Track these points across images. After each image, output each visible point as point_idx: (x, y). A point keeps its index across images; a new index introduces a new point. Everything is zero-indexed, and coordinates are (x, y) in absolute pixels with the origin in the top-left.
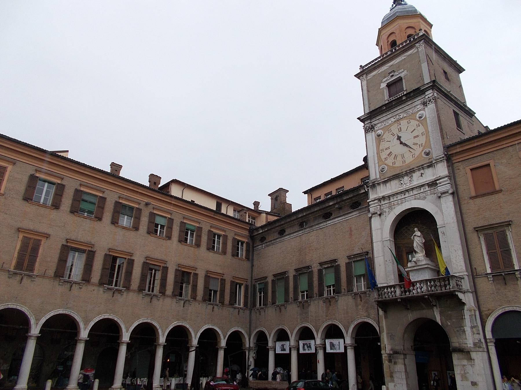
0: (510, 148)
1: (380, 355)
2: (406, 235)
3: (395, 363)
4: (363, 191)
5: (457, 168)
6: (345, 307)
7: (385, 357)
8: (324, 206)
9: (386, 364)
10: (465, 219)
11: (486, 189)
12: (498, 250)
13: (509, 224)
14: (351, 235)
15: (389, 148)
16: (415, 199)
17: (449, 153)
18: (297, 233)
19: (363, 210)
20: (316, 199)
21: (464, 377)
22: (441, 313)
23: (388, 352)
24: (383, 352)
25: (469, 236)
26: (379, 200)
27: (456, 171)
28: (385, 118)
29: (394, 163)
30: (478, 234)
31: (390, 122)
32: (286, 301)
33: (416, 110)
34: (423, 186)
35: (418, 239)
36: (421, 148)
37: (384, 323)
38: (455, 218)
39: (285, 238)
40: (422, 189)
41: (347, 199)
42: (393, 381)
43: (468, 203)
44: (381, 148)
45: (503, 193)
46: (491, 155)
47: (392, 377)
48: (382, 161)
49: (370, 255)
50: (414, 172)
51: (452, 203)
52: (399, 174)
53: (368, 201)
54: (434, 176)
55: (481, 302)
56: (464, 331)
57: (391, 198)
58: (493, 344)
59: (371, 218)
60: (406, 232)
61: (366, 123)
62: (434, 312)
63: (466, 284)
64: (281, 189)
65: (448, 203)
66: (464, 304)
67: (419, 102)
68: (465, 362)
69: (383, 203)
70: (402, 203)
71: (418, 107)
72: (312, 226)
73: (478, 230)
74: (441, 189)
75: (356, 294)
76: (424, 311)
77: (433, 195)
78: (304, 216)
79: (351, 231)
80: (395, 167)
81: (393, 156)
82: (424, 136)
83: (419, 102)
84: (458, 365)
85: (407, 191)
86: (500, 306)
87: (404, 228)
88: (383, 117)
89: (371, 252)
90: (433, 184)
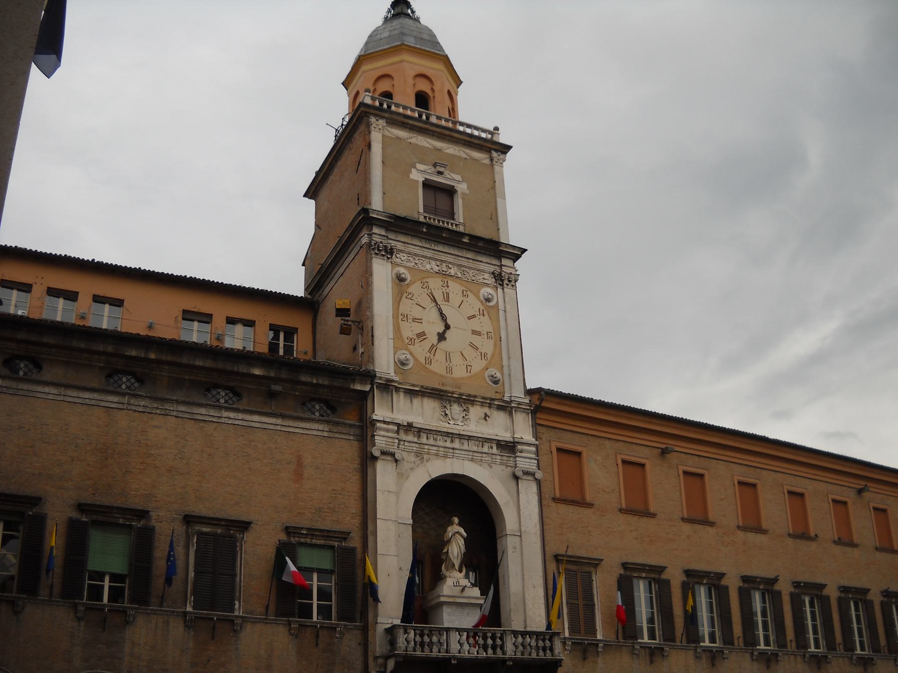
0: (607, 442)
4: (358, 387)
8: (229, 367)
12: (581, 603)
14: (298, 475)
16: (472, 460)
17: (544, 404)
18: (95, 396)
19: (341, 429)
28: (417, 251)
31: (428, 267)
33: (480, 278)
36: (484, 363)
39: (40, 388)
40: (486, 445)
50: (473, 405)
57: (424, 436)
59: (375, 459)
69: (403, 436)
70: (445, 457)
72: (163, 400)
77: (503, 467)
78: (147, 360)
79: (300, 464)
80: (430, 371)
81: (427, 345)
83: (492, 269)
85: (461, 437)
88: (415, 246)
90: (509, 447)
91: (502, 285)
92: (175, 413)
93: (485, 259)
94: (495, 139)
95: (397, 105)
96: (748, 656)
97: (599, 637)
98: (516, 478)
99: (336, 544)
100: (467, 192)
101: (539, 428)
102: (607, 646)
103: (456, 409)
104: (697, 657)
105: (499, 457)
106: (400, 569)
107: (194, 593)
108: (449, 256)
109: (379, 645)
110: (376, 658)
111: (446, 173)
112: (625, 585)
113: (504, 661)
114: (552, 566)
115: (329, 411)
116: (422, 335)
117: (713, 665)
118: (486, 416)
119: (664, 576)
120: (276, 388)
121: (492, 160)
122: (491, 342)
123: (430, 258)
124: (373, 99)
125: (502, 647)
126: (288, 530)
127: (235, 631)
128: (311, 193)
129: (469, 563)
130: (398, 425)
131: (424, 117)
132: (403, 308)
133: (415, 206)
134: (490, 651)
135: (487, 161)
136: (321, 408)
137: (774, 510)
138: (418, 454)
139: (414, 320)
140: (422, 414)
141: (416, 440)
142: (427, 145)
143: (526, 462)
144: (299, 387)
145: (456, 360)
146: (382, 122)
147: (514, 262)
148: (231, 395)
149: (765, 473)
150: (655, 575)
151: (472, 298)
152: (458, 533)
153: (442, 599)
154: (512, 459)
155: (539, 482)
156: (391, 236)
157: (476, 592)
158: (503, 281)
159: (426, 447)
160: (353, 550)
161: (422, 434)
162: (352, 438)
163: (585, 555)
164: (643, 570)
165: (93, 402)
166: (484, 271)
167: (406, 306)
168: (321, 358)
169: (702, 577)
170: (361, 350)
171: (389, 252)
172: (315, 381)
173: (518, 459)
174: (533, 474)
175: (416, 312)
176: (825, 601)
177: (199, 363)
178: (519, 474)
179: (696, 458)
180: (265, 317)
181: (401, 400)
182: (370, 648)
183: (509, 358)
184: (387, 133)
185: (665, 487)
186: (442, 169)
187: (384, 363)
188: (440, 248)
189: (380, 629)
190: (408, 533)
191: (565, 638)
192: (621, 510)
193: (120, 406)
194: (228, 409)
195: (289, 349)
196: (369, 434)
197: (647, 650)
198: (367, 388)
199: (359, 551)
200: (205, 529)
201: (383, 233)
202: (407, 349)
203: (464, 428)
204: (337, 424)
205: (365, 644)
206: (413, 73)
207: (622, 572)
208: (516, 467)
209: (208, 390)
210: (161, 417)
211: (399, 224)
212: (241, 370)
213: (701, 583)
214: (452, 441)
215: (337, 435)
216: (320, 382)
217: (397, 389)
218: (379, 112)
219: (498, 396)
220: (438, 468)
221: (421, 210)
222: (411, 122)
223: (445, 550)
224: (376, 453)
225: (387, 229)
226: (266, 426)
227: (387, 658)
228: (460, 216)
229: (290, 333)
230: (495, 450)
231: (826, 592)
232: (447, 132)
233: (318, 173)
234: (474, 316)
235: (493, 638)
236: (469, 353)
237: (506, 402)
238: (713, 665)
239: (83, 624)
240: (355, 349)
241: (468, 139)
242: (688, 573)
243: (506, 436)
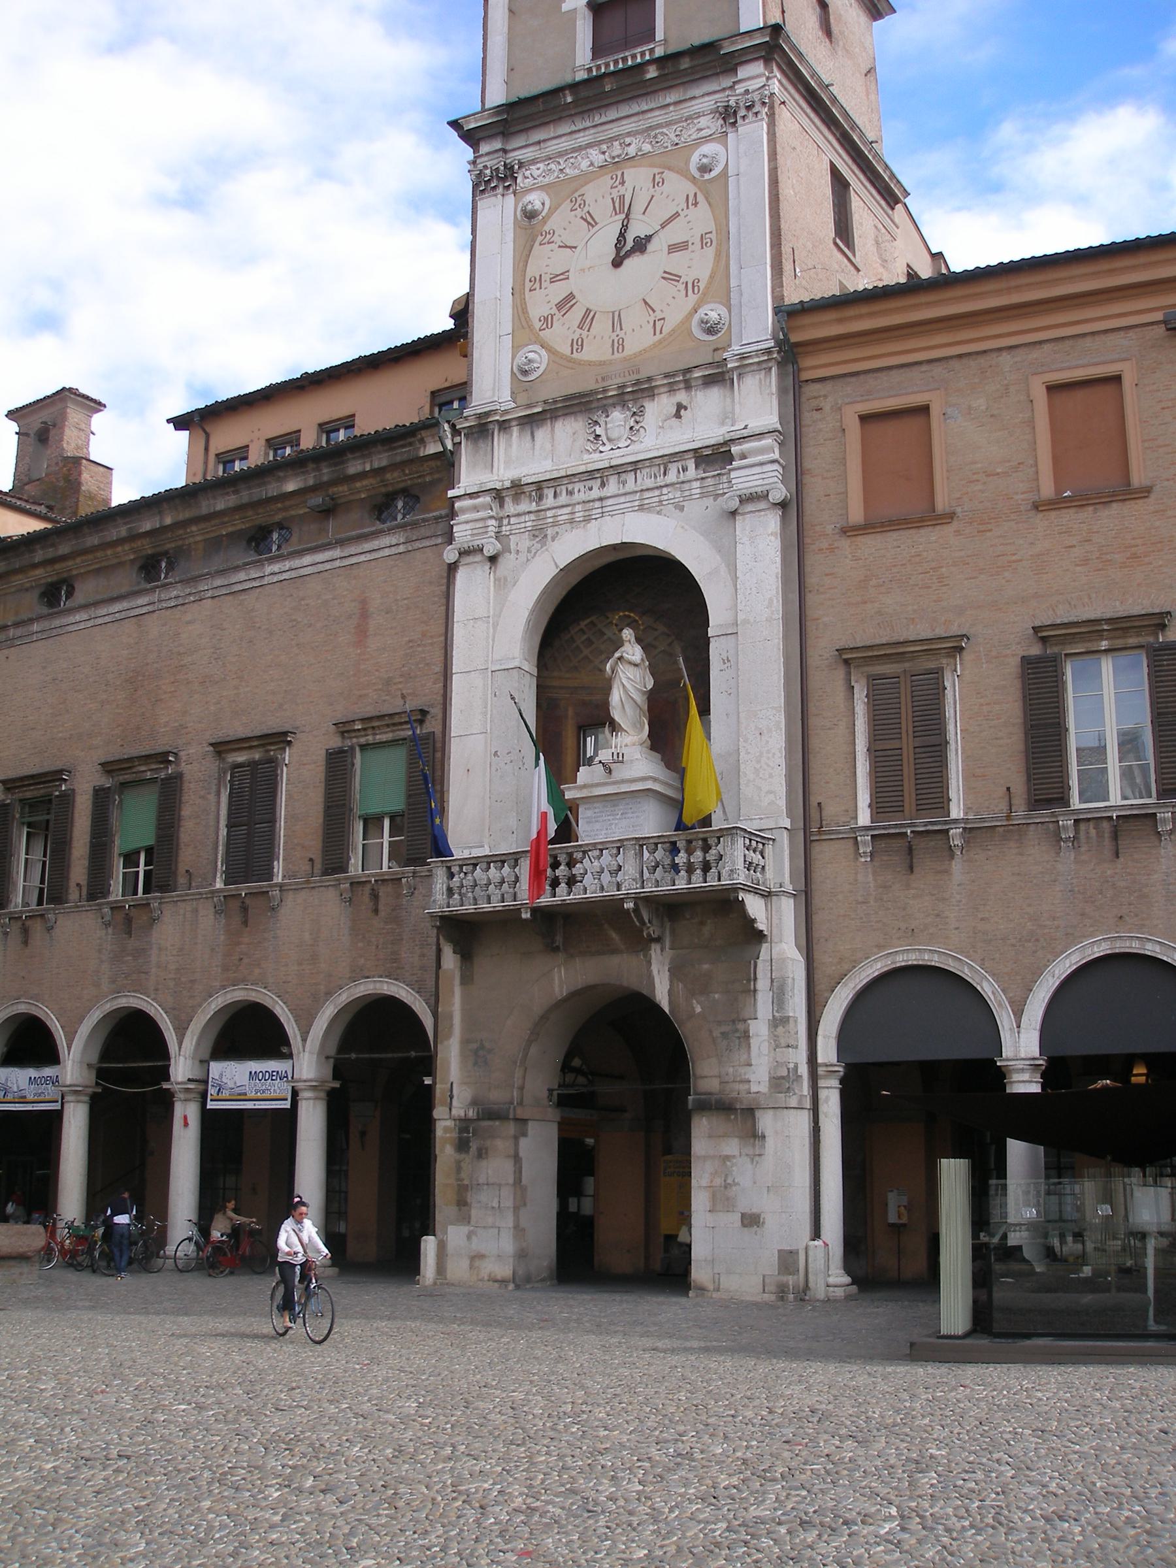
0: (1005, 358)
1: (428, 1124)
2: (586, 652)
3: (481, 1154)
4: (433, 448)
5: (814, 403)
6: (307, 936)
7: (446, 1129)
9: (445, 1154)
10: (811, 613)
11: (904, 498)
12: (907, 744)
13: (955, 647)
14: (362, 633)
15: (563, 276)
16: (641, 508)
17: (794, 338)
18: (125, 605)
19: (423, 531)
20: (226, 459)
21: (722, 1199)
22: (676, 972)
23: (458, 1112)
24: (439, 1112)
25: (816, 679)
26: (498, 495)
27: (808, 417)
28: (564, 144)
29: (578, 345)
30: (849, 674)
32: (53, 892)
33: (691, 134)
35: (629, 677)
36: (693, 298)
37: (455, 1003)
38: (778, 605)
39: (71, 619)
41: (363, 475)
42: (466, 1219)
43: (832, 549)
44: (532, 271)
45: (955, 525)
46: (938, 370)
47: (462, 1203)
49: (432, 725)
50: (652, 397)
51: (776, 543)
52: (592, 393)
53: (451, 493)
54: (723, 423)
55: (819, 932)
56: (746, 1036)
57: (549, 493)
58: (835, 1083)
59: (452, 568)
60: (589, 642)
61: (485, 148)
62: (649, 963)
63: (779, 867)
64: (65, 395)
65: (762, 543)
66: (760, 936)
67: (707, 104)
68: (731, 1147)
70: (587, 519)
71: (704, 122)
72: (195, 579)
73: (848, 659)
74: (744, 479)
75: (356, 884)
76: (614, 961)
77: (709, 501)
78: (164, 529)
79: (364, 615)
80: (579, 363)
81: (577, 314)
82: (710, 252)
84: (705, 1158)
85: (618, 470)
86: (880, 947)
87: (583, 624)
88: (559, 138)
89: (436, 711)
90: (716, 457)
92: (209, 594)
102: (970, 832)
105: (697, 484)
106: (496, 754)
140: (558, 449)
144: (358, 485)
152: (620, 658)
154: (724, 479)
158: (735, 113)
159: (549, 513)
161: (546, 491)
162: (439, 540)
164: (1100, 634)
165: (123, 615)
166: (699, 115)
173: (733, 475)
177: (220, 505)
188: (612, 114)
192: (1036, 507)
193: (150, 608)
197: (1105, 825)
199: (438, 735)
200: (241, 758)
204: (414, 525)
207: (1035, 650)
210: (195, 605)
214: (603, 485)
215: (418, 545)
216: (376, 465)
217: (504, 426)
226: (321, 567)
234: (677, 215)
239: (110, 930)
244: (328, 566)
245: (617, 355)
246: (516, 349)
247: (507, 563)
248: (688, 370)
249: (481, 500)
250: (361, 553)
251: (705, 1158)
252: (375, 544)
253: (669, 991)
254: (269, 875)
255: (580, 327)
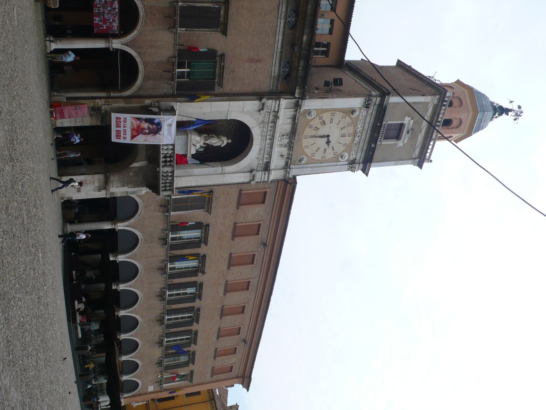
0: (269, 216)
3: (91, 115)
4: (297, 91)
7: (98, 103)
9: (91, 103)
14: (251, 61)
16: (260, 149)
17: (289, 185)
22: (140, 168)
23: (103, 107)
28: (368, 120)
31: (359, 126)
34: (270, 157)
36: (310, 155)
44: (337, 113)
48: (320, 114)
50: (288, 149)
56: (124, 186)
59: (260, 100)
65: (243, 178)
68: (97, 184)
70: (262, 136)
77: (257, 165)
81: (319, 126)
83: (358, 158)
84: (94, 178)
86: (143, 202)
90: (267, 168)
91: (349, 164)
93: (363, 155)
94: (426, 160)
95: (445, 110)
96: (163, 286)
97: (172, 213)
98: (251, 171)
99: (216, 80)
100: (398, 146)
101: (277, 182)
102: (167, 217)
103: (286, 141)
104: (162, 261)
107: (189, 7)
108: (365, 137)
109: (165, 103)
110: (158, 102)
111: (408, 135)
112: (198, 226)
113: (159, 167)
114: (207, 190)
115: (284, 76)
116: (324, 123)
117: (158, 269)
118: (282, 156)
119: (203, 245)
120: (296, 48)
121: (415, 159)
122: (320, 159)
123: (364, 127)
124: (449, 97)
125: (166, 166)
126: (223, 56)
127: (169, 29)
128: (400, 64)
129: (208, 148)
130: (278, 112)
131: (438, 124)
132: (338, 113)
133: (390, 120)
134: (164, 159)
135: (414, 156)
136: (286, 72)
137: (235, 299)
138: (263, 122)
139: (332, 119)
141: (270, 120)
142: (423, 125)
143: (260, 176)
145: (312, 140)
146: (436, 102)
147: (362, 170)
148: (292, 24)
149: (254, 294)
150: (203, 240)
151: (343, 148)
153: (189, 135)
155: (249, 182)
156: (376, 107)
157: (193, 152)
158: (351, 164)
160: (214, 90)
163: (213, 206)
164: (205, 235)
167: (339, 115)
168: (313, 70)
169: (202, 264)
170: (316, 92)
171: (367, 106)
172: (300, 68)
174: (253, 180)
175: (336, 120)
176: (190, 323)
177: (309, 7)
178: (253, 173)
179: (261, 261)
180: (334, 40)
181: (290, 113)
182: (164, 99)
183: (312, 167)
184: (430, 104)
185: (247, 245)
186: (410, 133)
187: (309, 104)
188: (369, 132)
189: (174, 104)
190: (223, 117)
191: (171, 196)
192: (235, 223)
194: (285, 23)
195: (317, 53)
196: (274, 97)
198: (297, 96)
200: (222, 12)
201: (377, 103)
202: (317, 115)
203: (277, 145)
204: (278, 80)
205: (166, 96)
206: (462, 118)
208: (257, 171)
209: (295, 12)
211: (381, 111)
212: (306, 29)
213: (199, 263)
214: (270, 139)
215: (272, 80)
216: (300, 71)
217: (296, 111)
218: (442, 101)
219: (293, 162)
220: (256, 132)
221: (389, 122)
222: (436, 117)
223: (214, 136)
224: (264, 100)
225: (379, 105)
226: (276, 43)
227: (159, 107)
228: (385, 142)
229: (326, 53)
230: (265, 160)
231: (195, 324)
232: (430, 135)
233: (410, 67)
234: (333, 149)
235: (170, 161)
236: (315, 147)
237: (290, 166)
238: (158, 269)
240: (317, 89)
241: (426, 147)
242: (204, 257)
243: (272, 166)
244: (276, 46)
245: (303, 137)
246: (316, 110)
247: (257, 115)
248: (291, 160)
249: (277, 108)
250: (276, 59)
251: (94, 178)
252: (277, 65)
253: (135, 167)
254: (180, 27)
255: (316, 127)
